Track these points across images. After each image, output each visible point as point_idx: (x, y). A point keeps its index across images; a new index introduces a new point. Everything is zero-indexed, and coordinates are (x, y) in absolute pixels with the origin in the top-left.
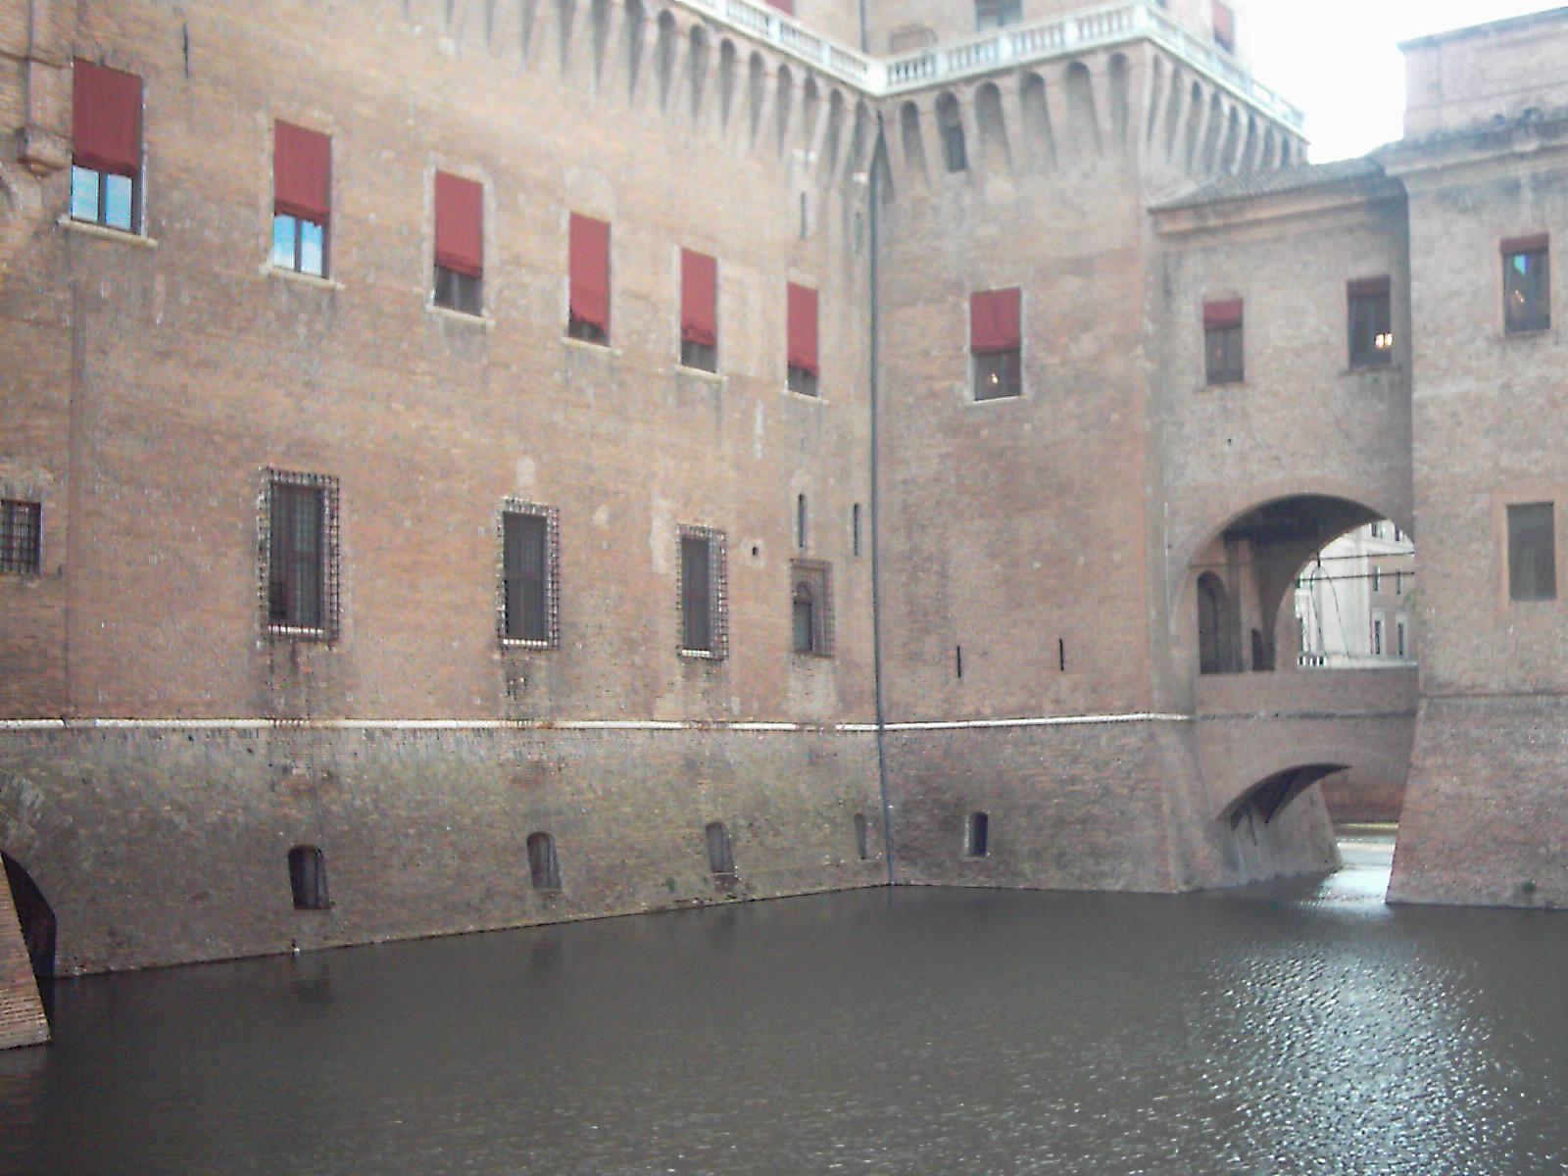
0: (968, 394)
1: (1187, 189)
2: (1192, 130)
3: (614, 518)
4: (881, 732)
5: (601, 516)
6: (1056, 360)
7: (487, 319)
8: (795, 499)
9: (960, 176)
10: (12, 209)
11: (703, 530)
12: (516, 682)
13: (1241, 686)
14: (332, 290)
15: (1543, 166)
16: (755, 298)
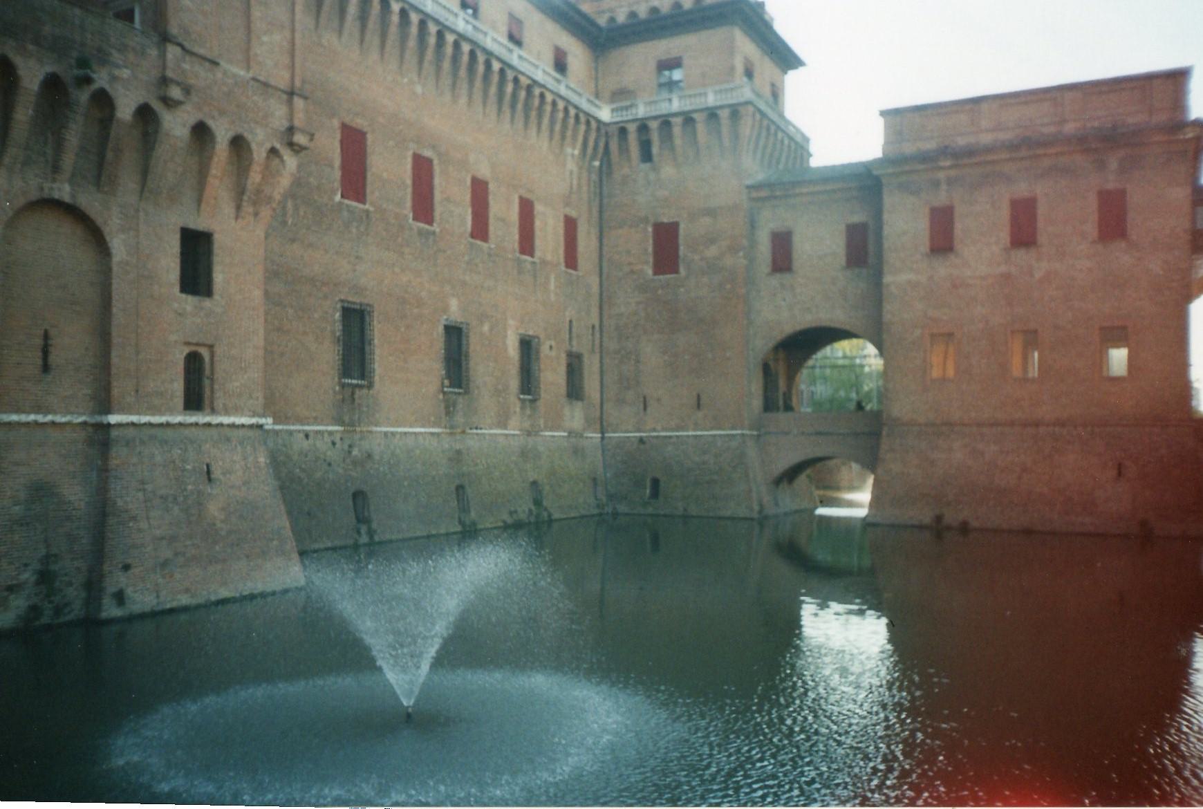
0: (650, 272)
1: (760, 177)
2: (765, 147)
3: (491, 329)
4: (603, 438)
5: (486, 328)
6: (697, 257)
7: (436, 228)
8: (568, 319)
9: (648, 165)
10: (284, 167)
11: (529, 336)
12: (450, 408)
13: (782, 417)
14: (367, 211)
15: (953, 173)
16: (551, 222)
